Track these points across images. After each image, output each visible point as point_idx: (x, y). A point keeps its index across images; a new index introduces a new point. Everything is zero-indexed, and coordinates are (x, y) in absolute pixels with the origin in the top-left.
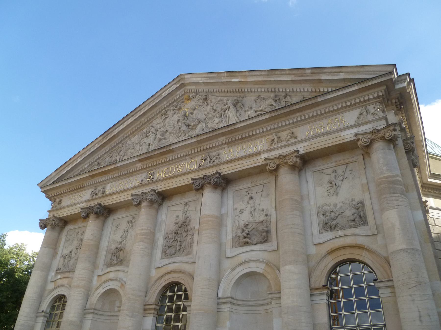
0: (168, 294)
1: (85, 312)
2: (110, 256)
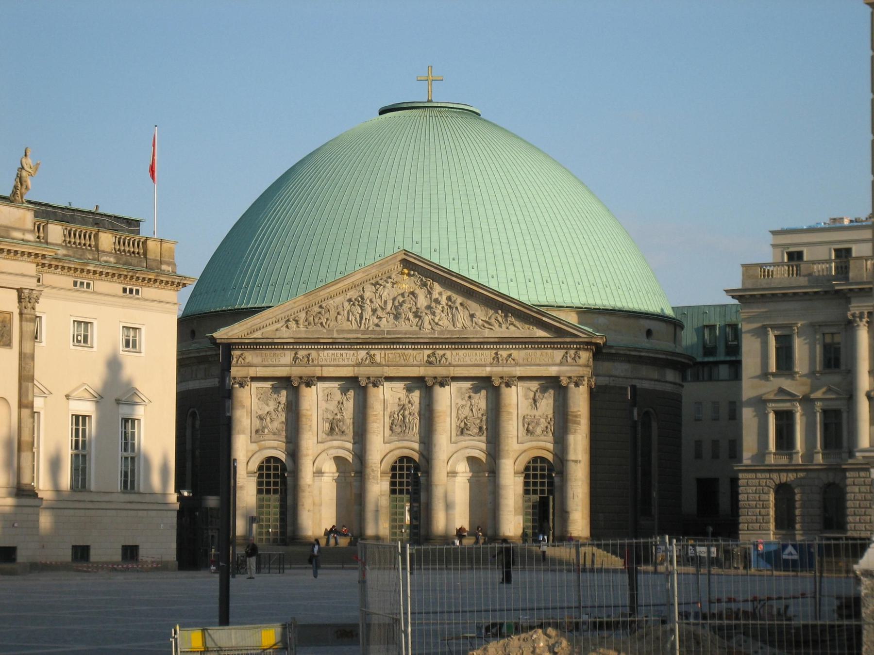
2: (327, 426)
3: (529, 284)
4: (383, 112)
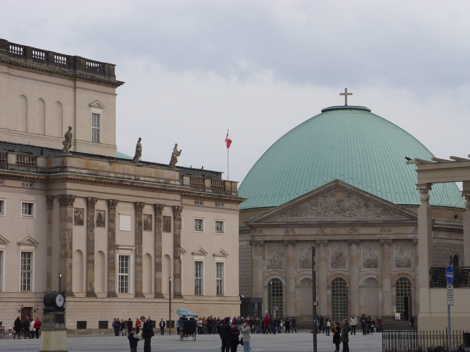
0: (335, 282)
1: (296, 287)
3: (396, 194)
4: (323, 111)
